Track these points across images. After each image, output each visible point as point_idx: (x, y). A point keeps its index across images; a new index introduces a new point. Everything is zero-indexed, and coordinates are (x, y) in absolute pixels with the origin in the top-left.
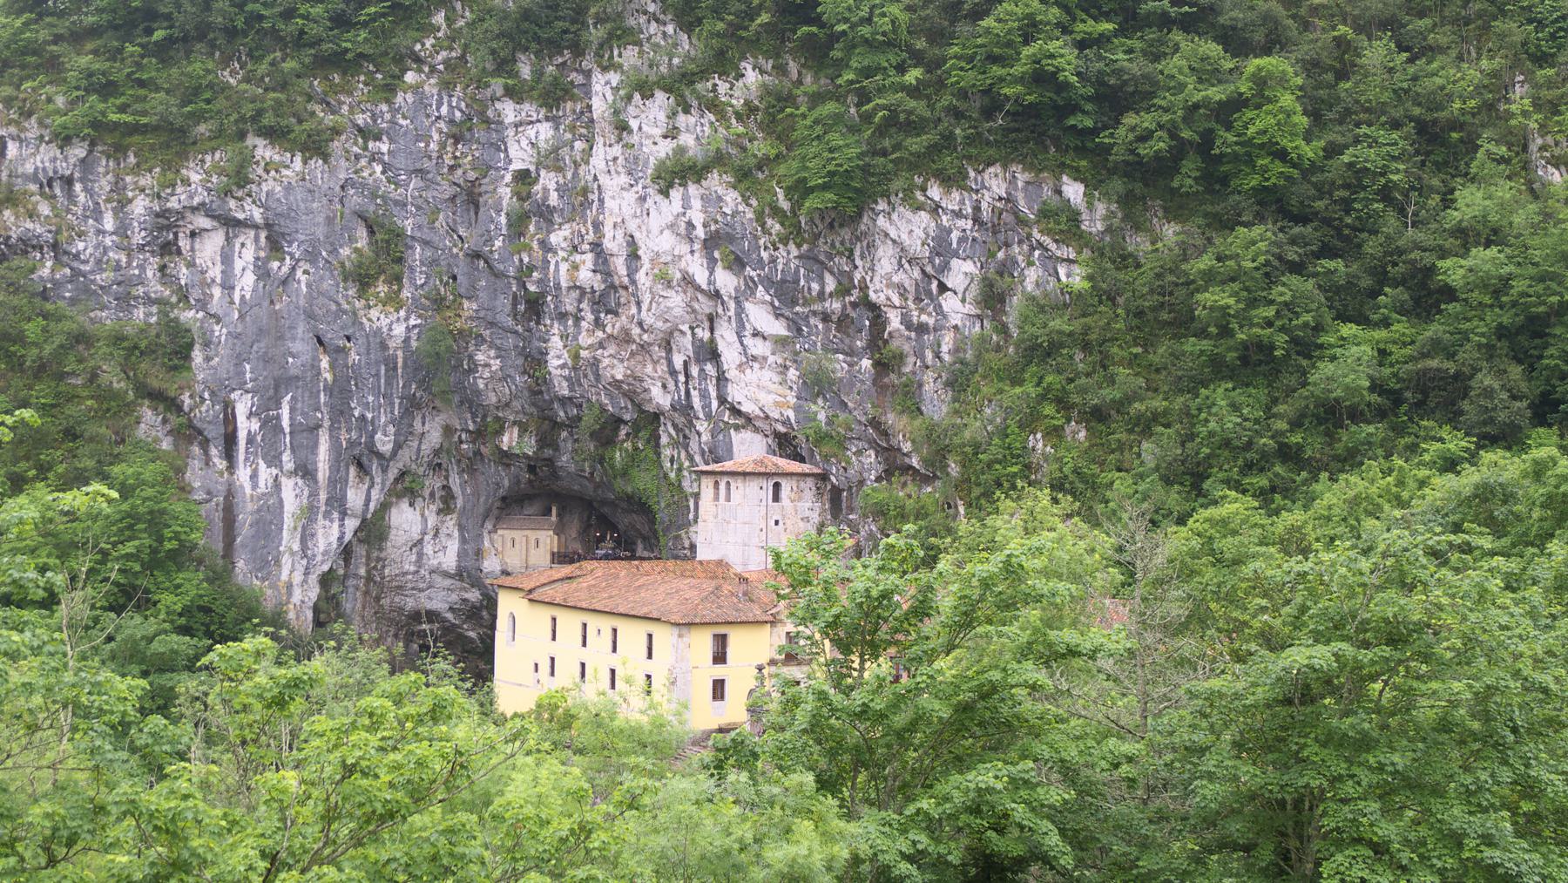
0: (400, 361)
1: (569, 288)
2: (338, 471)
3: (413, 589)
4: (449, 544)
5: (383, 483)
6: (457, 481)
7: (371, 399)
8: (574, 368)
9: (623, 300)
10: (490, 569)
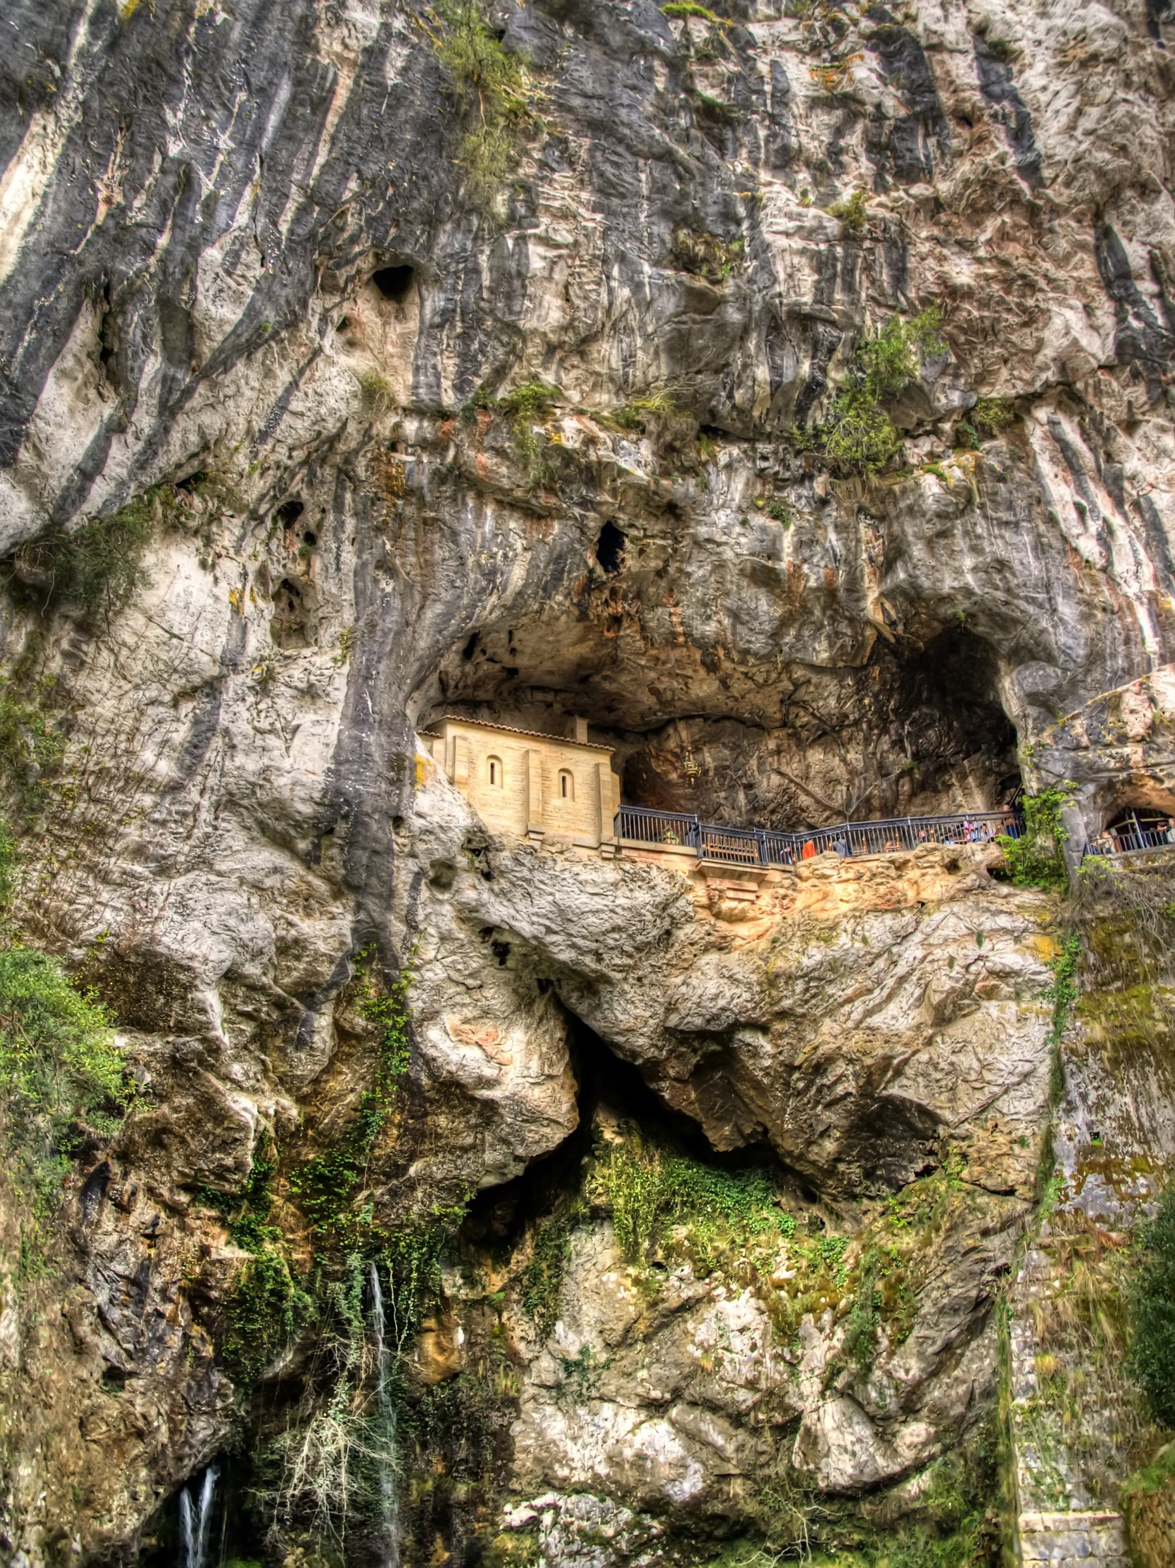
0: (340, 99)
1: (814, 103)
2: (48, 284)
3: (139, 852)
4: (306, 719)
5: (153, 445)
6: (349, 558)
7: (225, 141)
8: (849, 237)
9: (955, 143)
10: (436, 819)
